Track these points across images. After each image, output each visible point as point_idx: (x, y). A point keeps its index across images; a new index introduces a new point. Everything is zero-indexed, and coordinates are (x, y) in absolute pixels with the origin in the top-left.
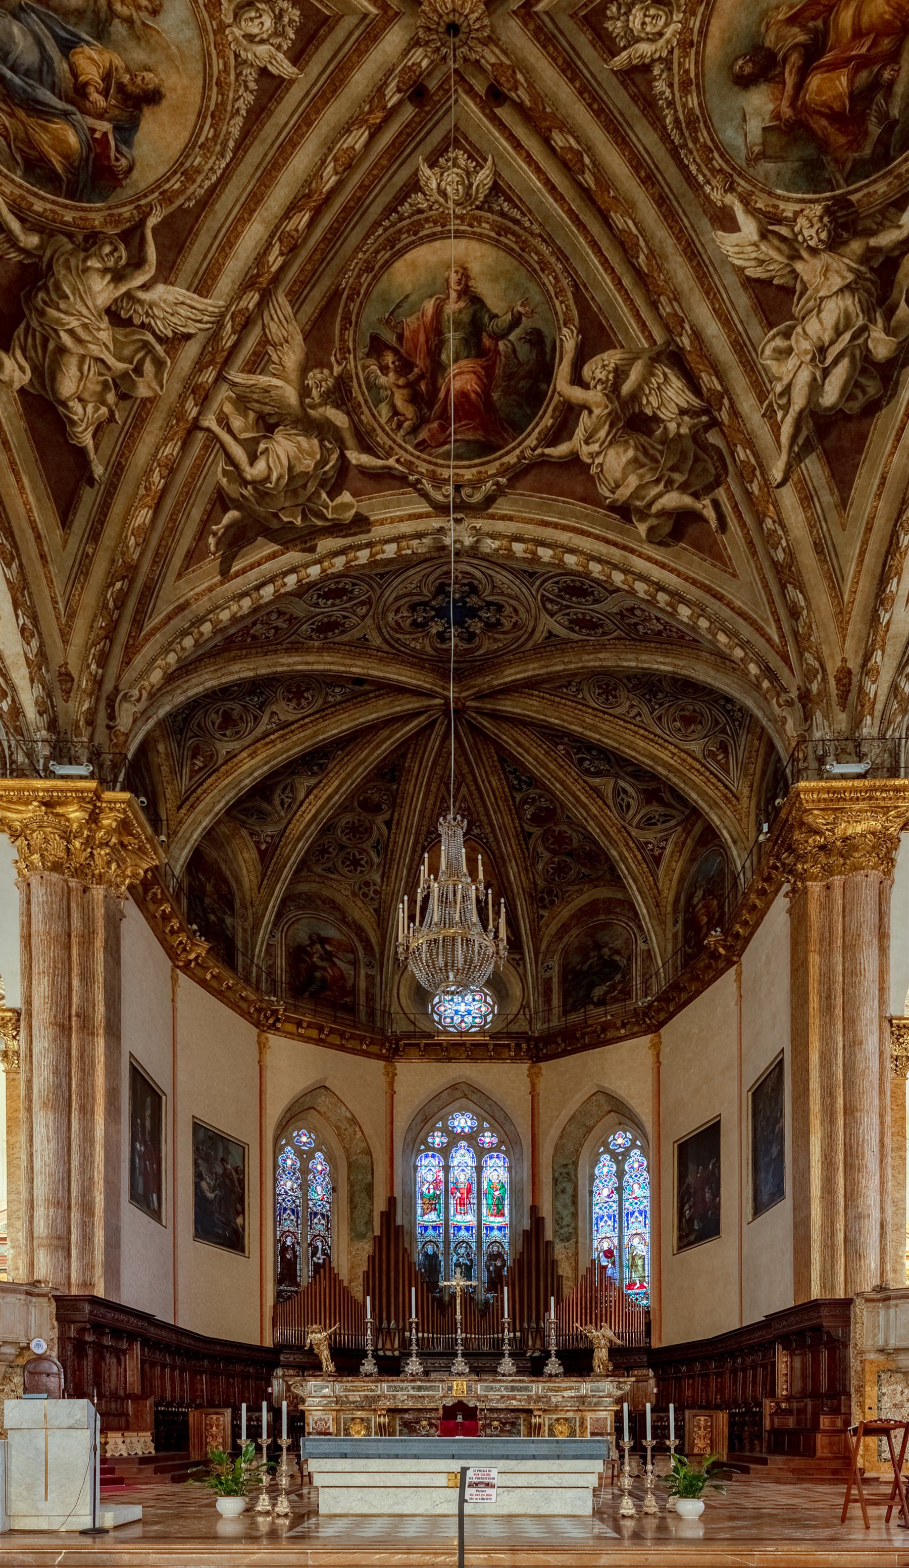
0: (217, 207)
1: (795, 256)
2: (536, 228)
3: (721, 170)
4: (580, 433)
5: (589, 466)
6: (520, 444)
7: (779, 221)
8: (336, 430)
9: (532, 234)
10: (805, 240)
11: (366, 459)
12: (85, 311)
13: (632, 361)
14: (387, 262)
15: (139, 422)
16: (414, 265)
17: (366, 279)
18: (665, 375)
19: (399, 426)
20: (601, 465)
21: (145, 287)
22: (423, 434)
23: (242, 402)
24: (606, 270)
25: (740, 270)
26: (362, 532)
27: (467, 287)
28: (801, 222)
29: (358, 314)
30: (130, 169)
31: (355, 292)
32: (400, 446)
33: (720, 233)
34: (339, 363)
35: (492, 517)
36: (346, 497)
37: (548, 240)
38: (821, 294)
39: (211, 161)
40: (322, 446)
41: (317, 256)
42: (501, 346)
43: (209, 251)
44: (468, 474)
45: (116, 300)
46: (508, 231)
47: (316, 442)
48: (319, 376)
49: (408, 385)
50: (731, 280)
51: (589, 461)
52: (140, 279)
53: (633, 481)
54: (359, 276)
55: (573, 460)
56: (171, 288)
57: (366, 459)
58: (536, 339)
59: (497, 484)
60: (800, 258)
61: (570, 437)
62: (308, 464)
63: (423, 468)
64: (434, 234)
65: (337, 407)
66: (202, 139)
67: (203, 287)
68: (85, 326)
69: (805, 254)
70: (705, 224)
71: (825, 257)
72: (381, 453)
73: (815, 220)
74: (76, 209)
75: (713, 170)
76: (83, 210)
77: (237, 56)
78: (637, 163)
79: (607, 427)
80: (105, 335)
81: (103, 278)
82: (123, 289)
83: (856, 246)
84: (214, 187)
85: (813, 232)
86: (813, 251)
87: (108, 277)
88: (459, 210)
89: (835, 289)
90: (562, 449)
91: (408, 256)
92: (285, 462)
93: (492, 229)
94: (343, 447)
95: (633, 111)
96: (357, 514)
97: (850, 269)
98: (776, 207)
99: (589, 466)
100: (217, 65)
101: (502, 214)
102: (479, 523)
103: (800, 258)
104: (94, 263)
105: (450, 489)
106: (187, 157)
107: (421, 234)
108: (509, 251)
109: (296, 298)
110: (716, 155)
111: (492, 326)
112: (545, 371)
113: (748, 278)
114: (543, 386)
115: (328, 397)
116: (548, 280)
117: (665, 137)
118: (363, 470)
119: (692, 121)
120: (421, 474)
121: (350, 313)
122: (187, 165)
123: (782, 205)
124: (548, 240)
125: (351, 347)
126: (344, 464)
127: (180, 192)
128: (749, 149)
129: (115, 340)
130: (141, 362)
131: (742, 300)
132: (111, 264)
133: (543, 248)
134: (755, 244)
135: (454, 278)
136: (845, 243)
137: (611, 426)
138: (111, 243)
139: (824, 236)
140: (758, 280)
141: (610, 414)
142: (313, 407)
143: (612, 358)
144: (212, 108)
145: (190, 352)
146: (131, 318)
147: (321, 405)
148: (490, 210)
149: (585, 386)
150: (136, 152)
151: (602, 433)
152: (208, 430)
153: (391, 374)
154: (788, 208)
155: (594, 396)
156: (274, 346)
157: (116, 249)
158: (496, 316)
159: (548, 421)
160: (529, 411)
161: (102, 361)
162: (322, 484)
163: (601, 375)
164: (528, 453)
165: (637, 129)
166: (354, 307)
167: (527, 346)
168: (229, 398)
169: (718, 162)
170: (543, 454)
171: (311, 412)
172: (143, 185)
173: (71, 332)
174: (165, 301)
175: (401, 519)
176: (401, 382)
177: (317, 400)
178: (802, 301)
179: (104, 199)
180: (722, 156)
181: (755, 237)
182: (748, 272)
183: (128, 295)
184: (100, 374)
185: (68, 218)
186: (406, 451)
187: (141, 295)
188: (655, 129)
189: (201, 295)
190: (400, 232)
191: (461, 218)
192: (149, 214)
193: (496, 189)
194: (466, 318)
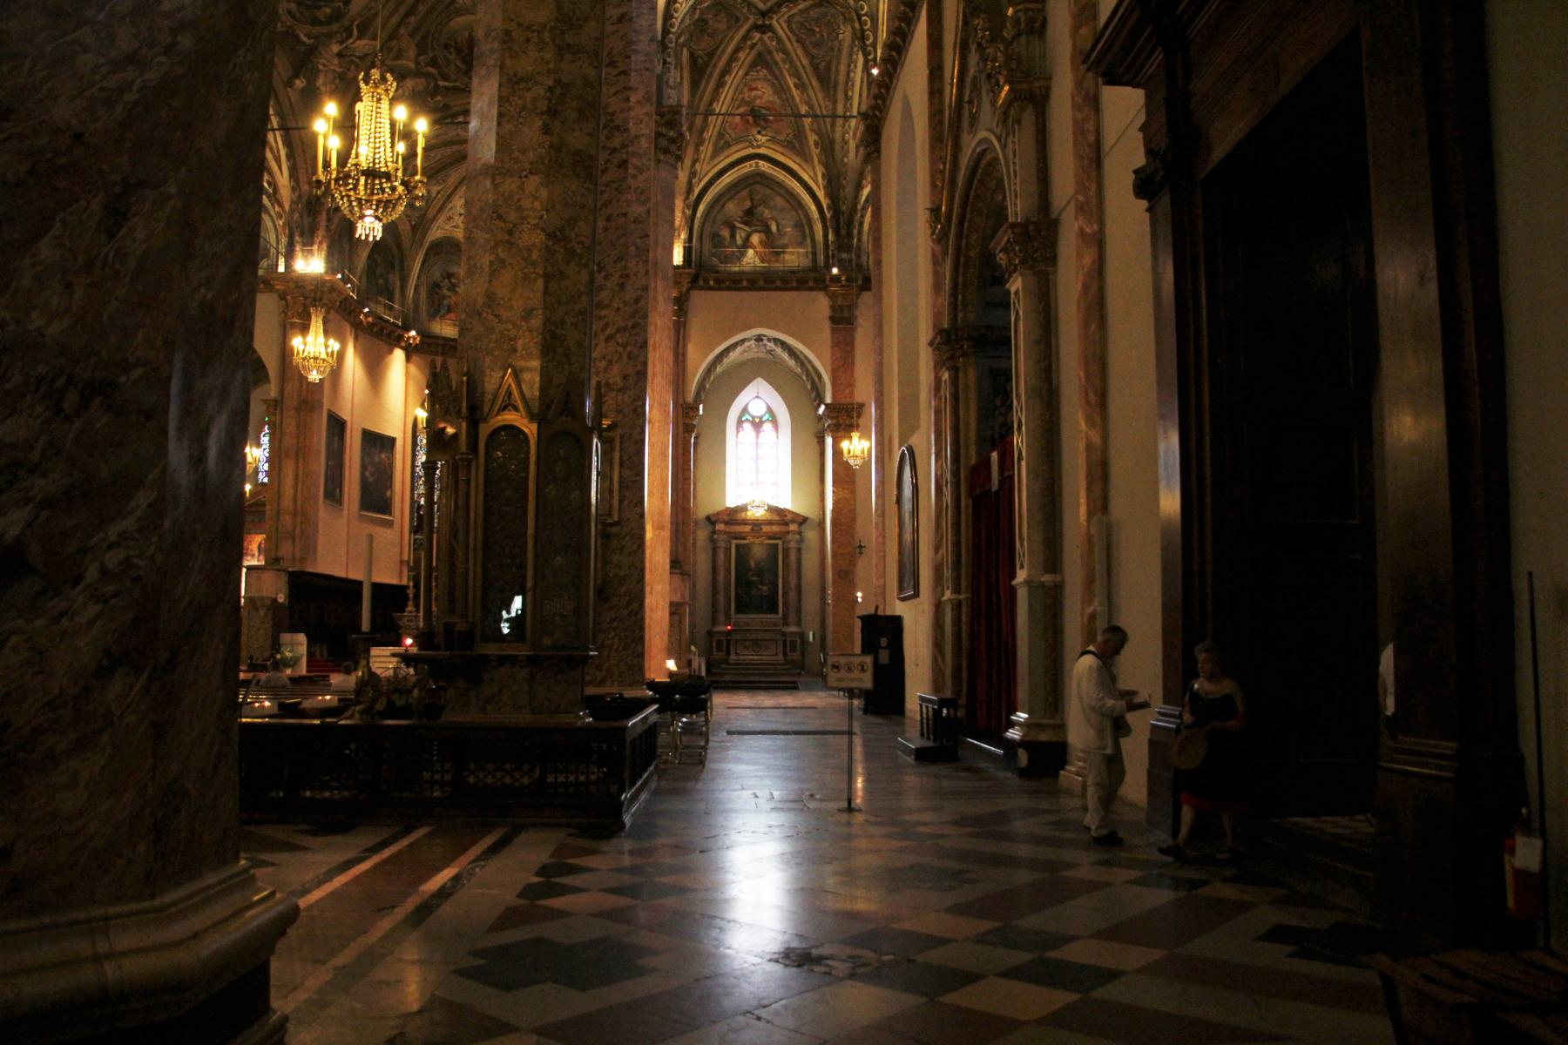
11: (446, 84)
36: (439, 98)
52: (351, 41)
57: (446, 84)
62: (422, 88)
94: (436, 80)
118: (443, 87)
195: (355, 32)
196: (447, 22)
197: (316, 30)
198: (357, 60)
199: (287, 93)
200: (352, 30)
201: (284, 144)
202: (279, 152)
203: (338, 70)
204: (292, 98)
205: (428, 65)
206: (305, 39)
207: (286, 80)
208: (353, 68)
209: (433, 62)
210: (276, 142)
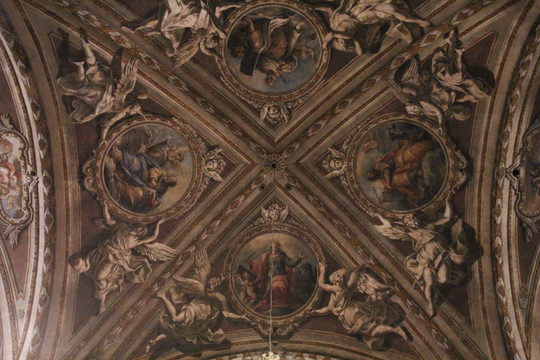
0: (186, 219)
1: (407, 231)
2: (305, 228)
3: (371, 206)
4: (331, 303)
5: (337, 317)
6: (304, 309)
7: (398, 220)
8: (219, 302)
9: (304, 230)
10: (410, 225)
11: (231, 315)
12: (123, 248)
13: (349, 273)
14: (248, 240)
15: (129, 293)
16: (258, 242)
17: (239, 246)
18: (366, 277)
19: (249, 301)
20: (343, 316)
21: (151, 243)
22: (259, 305)
23: (179, 288)
24: (334, 241)
25: (387, 238)
26: (225, 349)
27: (279, 248)
28: (406, 220)
29: (234, 258)
30: (158, 205)
31: (234, 250)
32: (248, 310)
33: (376, 226)
34: (224, 276)
35: (292, 342)
36: (220, 331)
37: (310, 232)
38: (423, 243)
40: (212, 308)
41: (221, 237)
42: (293, 270)
43: (179, 233)
44: (280, 322)
45: (137, 246)
46: (294, 230)
47: (209, 307)
48: (215, 280)
49: (254, 285)
50: (385, 241)
51: (337, 314)
53: (360, 322)
54: (236, 244)
55: (330, 314)
56: (161, 244)
58: (308, 267)
59: (294, 326)
60: (410, 231)
61: (327, 305)
62: (204, 316)
63: (258, 319)
64: (266, 231)
65: (221, 292)
66: (186, 198)
67: (173, 245)
68: (121, 254)
69: (411, 230)
70: (370, 224)
71: (420, 230)
72: (239, 312)
73: (411, 219)
74: (134, 215)
75: (367, 206)
76: (136, 215)
77: (204, 174)
78: (340, 206)
79: (343, 299)
80: (128, 258)
81: (135, 238)
82: (141, 243)
83: (430, 226)
84: (187, 212)
85: (412, 222)
86: (415, 229)
87: (137, 238)
88: (276, 223)
89: (428, 240)
90: (323, 310)
91: (256, 238)
92: (193, 315)
93: (288, 229)
95: (336, 190)
96: (225, 340)
97: (431, 233)
98: (395, 216)
99: (337, 317)
100: (197, 176)
101: (292, 224)
102: (285, 345)
103: (410, 231)
104: (133, 233)
105: (271, 329)
106: (179, 203)
107: (261, 231)
108: (295, 236)
109: (210, 251)
110: (368, 201)
111: (290, 263)
112: (313, 279)
113: (392, 240)
114: (313, 285)
115: (217, 289)
116: (311, 246)
117: (348, 197)
118: (229, 319)
119: (357, 192)
120: (258, 322)
121: (231, 257)
122: (179, 205)
123: (397, 215)
124: (310, 232)
125: (230, 270)
126: (221, 315)
127: (174, 213)
128: (379, 199)
129: (131, 260)
130: (140, 269)
131: (392, 247)
132: (140, 234)
133: (308, 235)
134: (390, 228)
135: (274, 246)
136: (426, 225)
137: (345, 299)
138: (142, 227)
139: (416, 223)
140: (396, 240)
141: (344, 294)
142: (210, 292)
143: (341, 272)
144: (192, 188)
145: (162, 267)
146: (141, 253)
147: (214, 292)
148: (288, 223)
149: (331, 284)
150: (162, 200)
151: (342, 302)
152: (161, 299)
153: (246, 281)
154: (400, 216)
155: (335, 287)
156: (198, 268)
157: (143, 229)
158: (291, 259)
159: (316, 298)
160: (307, 294)
161: (123, 267)
162: (209, 325)
163: (337, 279)
164: (308, 312)
165: (339, 195)
166: (233, 256)
167: (305, 270)
168: (173, 287)
169: (369, 203)
170: (315, 313)
171: (209, 294)
172: (161, 210)
173: (114, 255)
174: (157, 249)
175: (246, 343)
176: (250, 284)
177: (213, 290)
178: (416, 246)
179: (145, 213)
180: (370, 202)
181: (390, 226)
182: (391, 238)
183: (143, 245)
184: (120, 272)
185: (129, 217)
186: (251, 312)
188: (345, 195)
190: (253, 230)
191: (277, 226)
192: (160, 220)
193: (289, 216)
194: (279, 260)
195: (157, 232)
196: (248, 241)
197: (122, 211)
198: (149, 265)
199: (66, 270)
200: (155, 228)
201: (36, 324)
202: (23, 343)
203: (126, 267)
204: (68, 279)
205: (217, 289)
206: (108, 216)
207: (70, 254)
208: (142, 272)
209: (223, 288)
210: (26, 329)
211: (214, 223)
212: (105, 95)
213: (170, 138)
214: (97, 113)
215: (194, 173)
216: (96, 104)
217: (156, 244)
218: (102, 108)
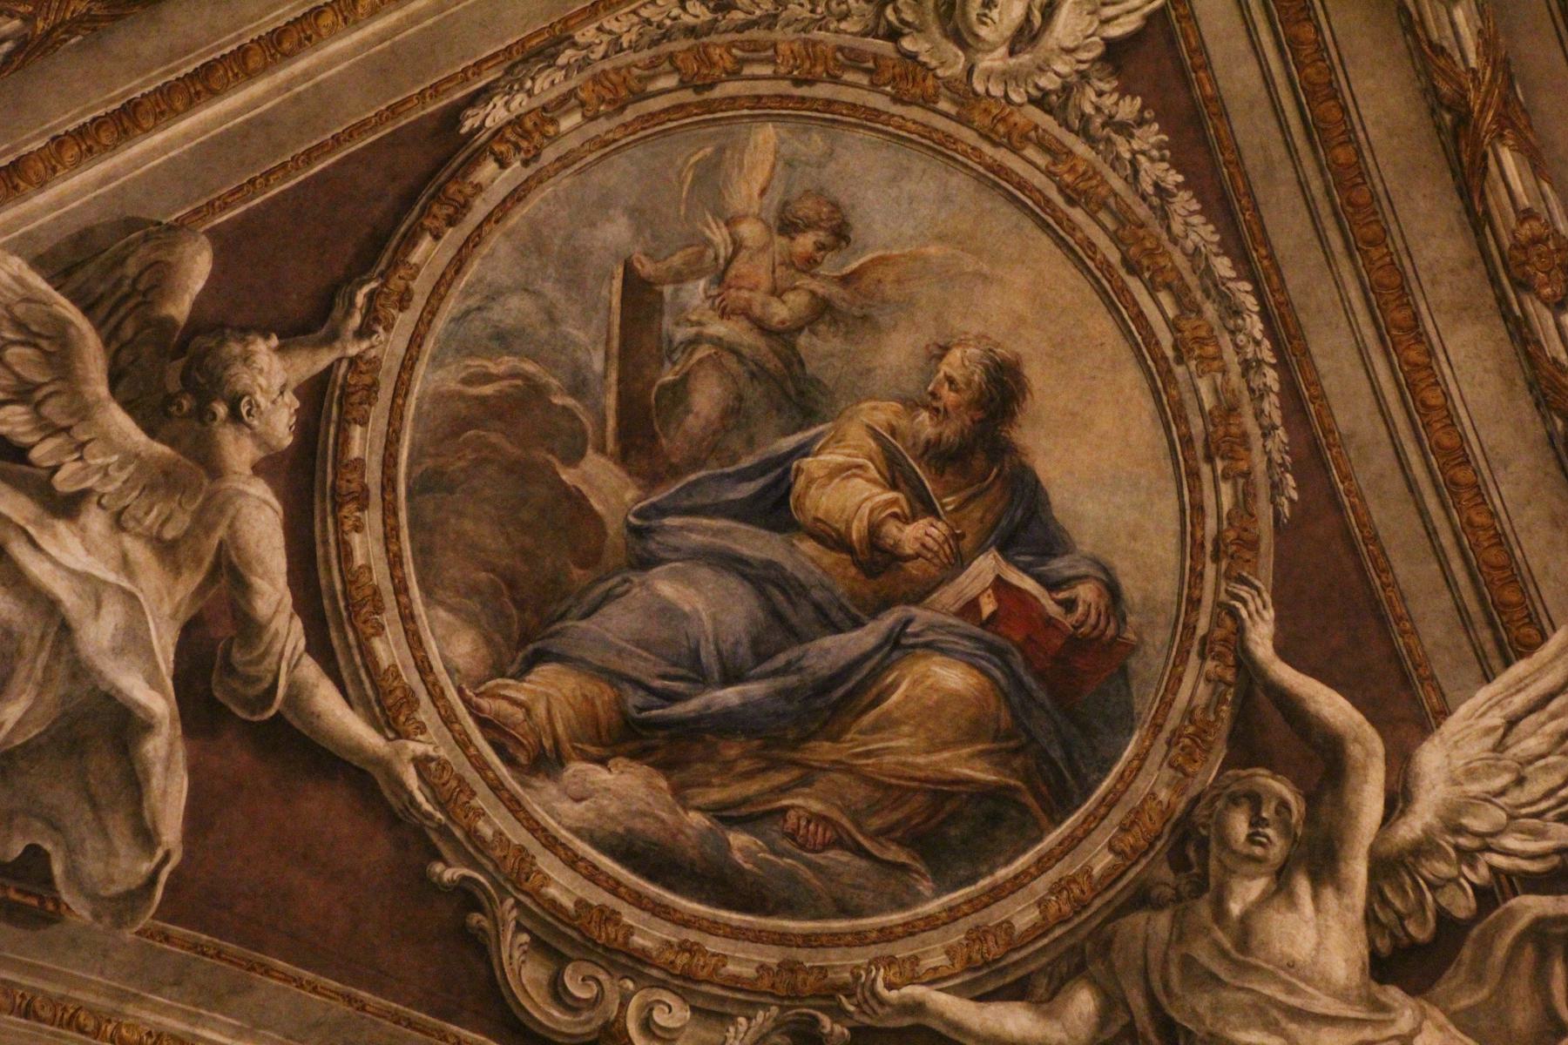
0: (1342, 420)
21: (1398, 800)
30: (1112, 590)
39: (1229, 354)
43: (1431, 533)
45: (1370, 918)
56: (1451, 725)
66: (1166, 340)
74: (1096, 818)
76: (1109, 803)
77: (1040, 101)
81: (1292, 903)
82: (1358, 870)
84: (1290, 392)
87: (1303, 887)
100: (1028, 166)
104: (1246, 893)
106: (1181, 418)
122: (1197, 426)
127: (1245, 499)
138: (1234, 801)
144: (1114, 257)
146: (1443, 916)
150: (1086, 540)
157: (1255, 800)
172: (1166, 588)
174: (1471, 774)
179: (1125, 722)
183: (1385, 867)
185: (1102, 861)
187: (1410, 829)
189: (1526, 649)
192: (1240, 630)
200: (1289, 706)
211: (1498, 200)
212: (37, 568)
213: (616, 232)
214: (158, 703)
215: (996, 180)
216: (80, 670)
217: (1432, 759)
218: (134, 641)
